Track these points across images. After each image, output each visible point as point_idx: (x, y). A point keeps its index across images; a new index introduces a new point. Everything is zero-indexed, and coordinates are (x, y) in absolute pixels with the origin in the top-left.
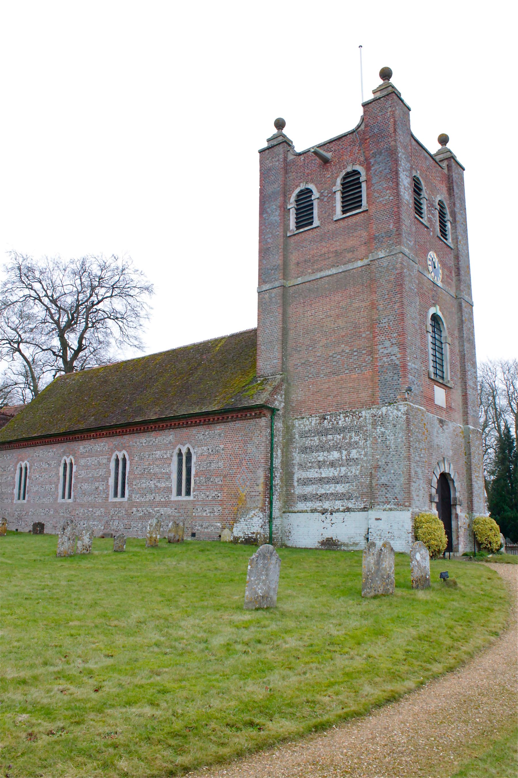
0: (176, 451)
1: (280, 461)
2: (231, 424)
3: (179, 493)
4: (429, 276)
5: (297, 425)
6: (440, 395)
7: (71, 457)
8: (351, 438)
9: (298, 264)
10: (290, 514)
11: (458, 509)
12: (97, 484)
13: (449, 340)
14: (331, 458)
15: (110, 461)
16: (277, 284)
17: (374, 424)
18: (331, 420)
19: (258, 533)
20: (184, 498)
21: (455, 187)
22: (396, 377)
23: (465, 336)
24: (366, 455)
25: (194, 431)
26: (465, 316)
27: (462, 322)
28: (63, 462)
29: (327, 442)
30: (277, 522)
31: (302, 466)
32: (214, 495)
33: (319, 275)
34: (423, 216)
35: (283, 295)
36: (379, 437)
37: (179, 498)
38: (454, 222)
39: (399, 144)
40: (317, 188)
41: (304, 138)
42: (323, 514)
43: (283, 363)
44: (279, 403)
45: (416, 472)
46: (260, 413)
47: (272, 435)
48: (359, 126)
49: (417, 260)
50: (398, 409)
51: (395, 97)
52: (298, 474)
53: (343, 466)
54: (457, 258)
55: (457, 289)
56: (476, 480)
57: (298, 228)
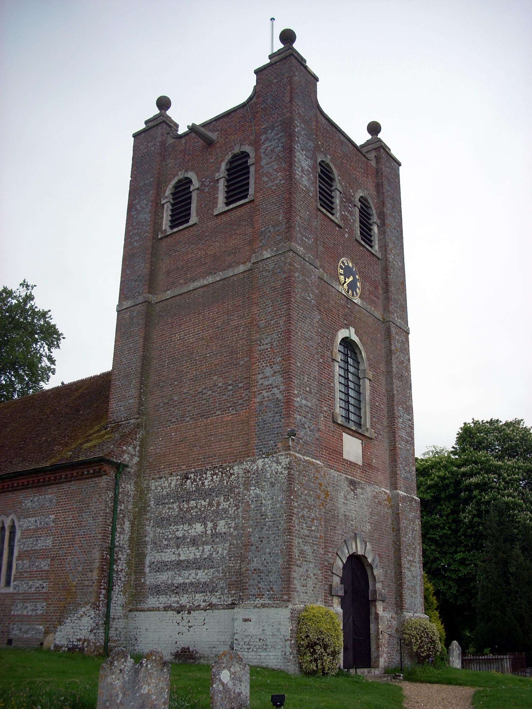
1: (127, 537)
2: (65, 486)
4: (340, 288)
5: (153, 488)
6: (352, 448)
8: (218, 504)
9: (168, 273)
10: (137, 613)
11: (380, 608)
13: (370, 374)
14: (193, 532)
16: (140, 299)
17: (247, 485)
18: (195, 480)
19: (85, 640)
21: (385, 183)
22: (277, 418)
23: (394, 370)
24: (235, 529)
25: (20, 496)
26: (396, 345)
27: (390, 353)
29: (189, 510)
30: (117, 625)
31: (158, 547)
32: (38, 585)
34: (334, 212)
35: (147, 313)
36: (252, 501)
38: (382, 226)
39: (296, 117)
40: (198, 176)
41: (185, 116)
42: (179, 612)
43: (141, 404)
44: (129, 455)
45: (302, 552)
46: (100, 469)
47: (116, 500)
48: (250, 99)
49: (318, 263)
50: (278, 463)
51: (294, 61)
52: (152, 557)
53: (207, 544)
54: (386, 270)
55: (384, 310)
56: (407, 565)
57: (172, 227)
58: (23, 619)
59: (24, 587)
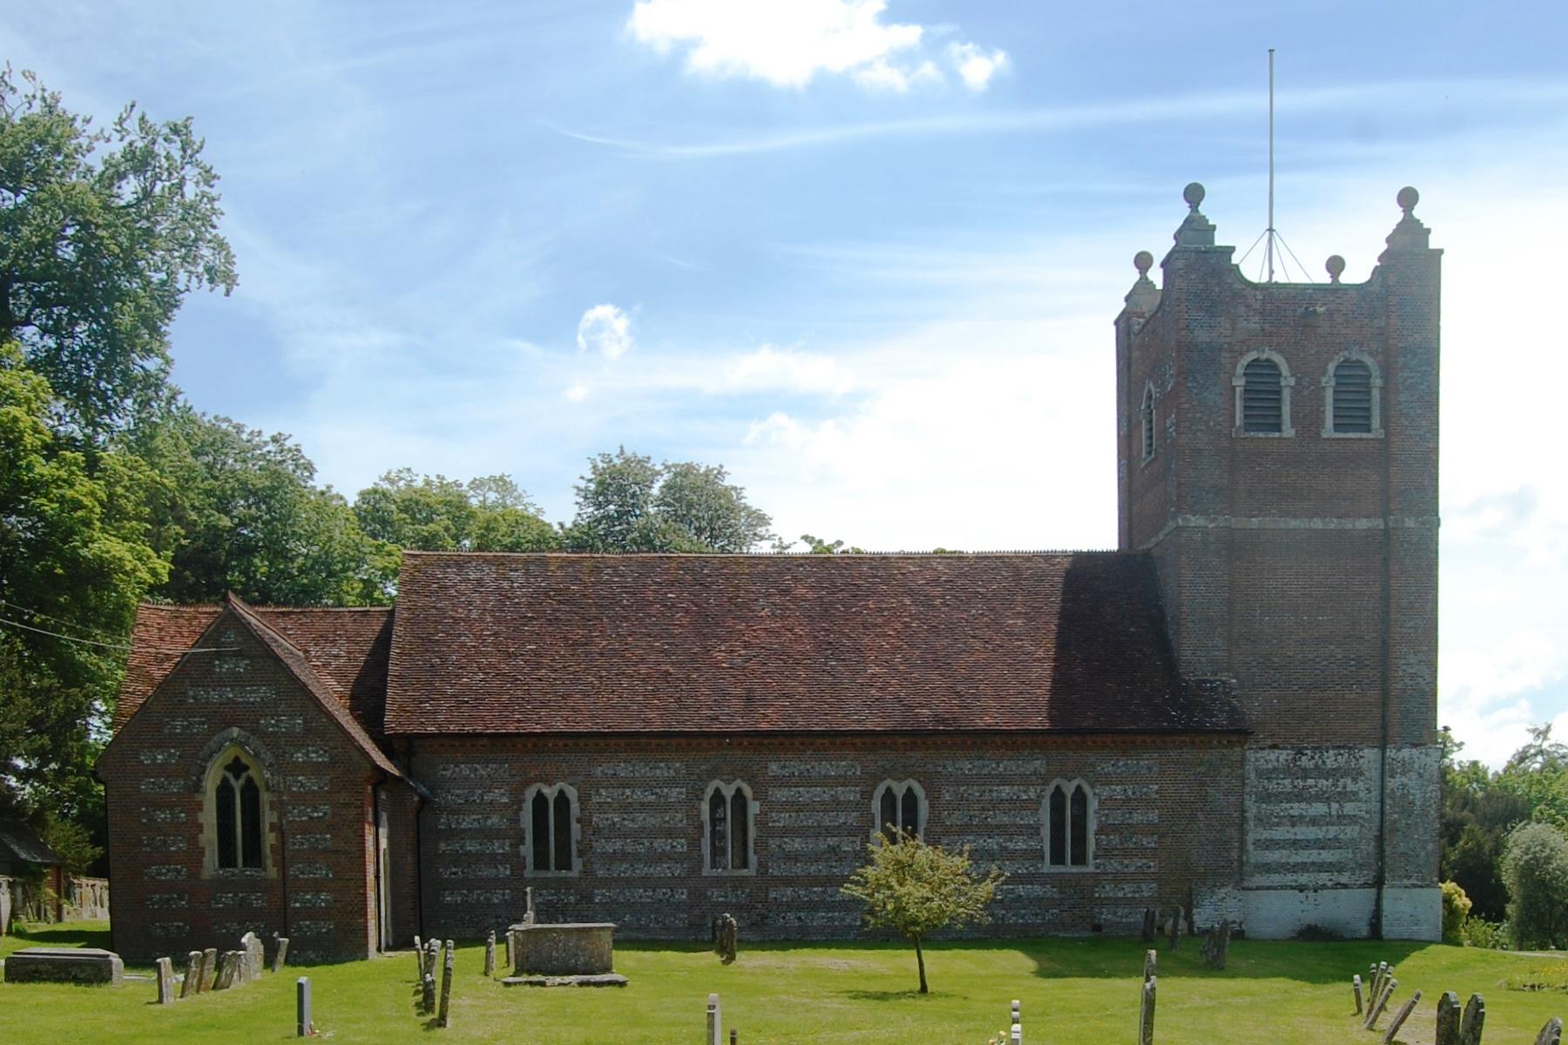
0: (1050, 789)
3: (1057, 858)
7: (739, 783)
12: (832, 841)
15: (871, 798)
20: (1069, 868)
28: (709, 792)
31: (1260, 821)
33: (1294, 523)
37: (1060, 869)
52: (1254, 833)
57: (1248, 427)
58: (1117, 902)
59: (1114, 865)
